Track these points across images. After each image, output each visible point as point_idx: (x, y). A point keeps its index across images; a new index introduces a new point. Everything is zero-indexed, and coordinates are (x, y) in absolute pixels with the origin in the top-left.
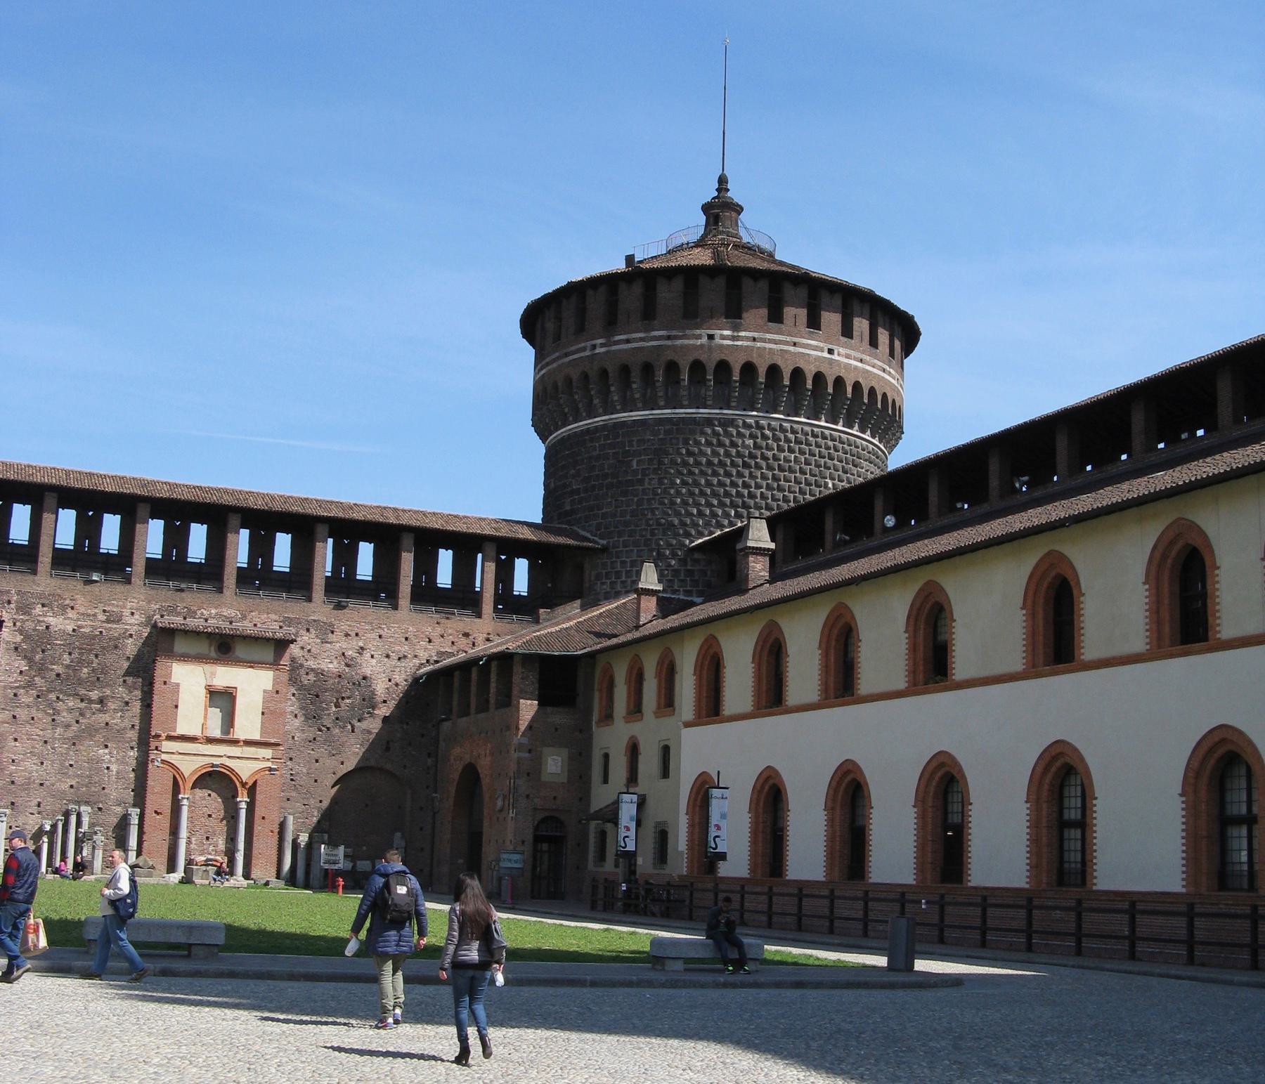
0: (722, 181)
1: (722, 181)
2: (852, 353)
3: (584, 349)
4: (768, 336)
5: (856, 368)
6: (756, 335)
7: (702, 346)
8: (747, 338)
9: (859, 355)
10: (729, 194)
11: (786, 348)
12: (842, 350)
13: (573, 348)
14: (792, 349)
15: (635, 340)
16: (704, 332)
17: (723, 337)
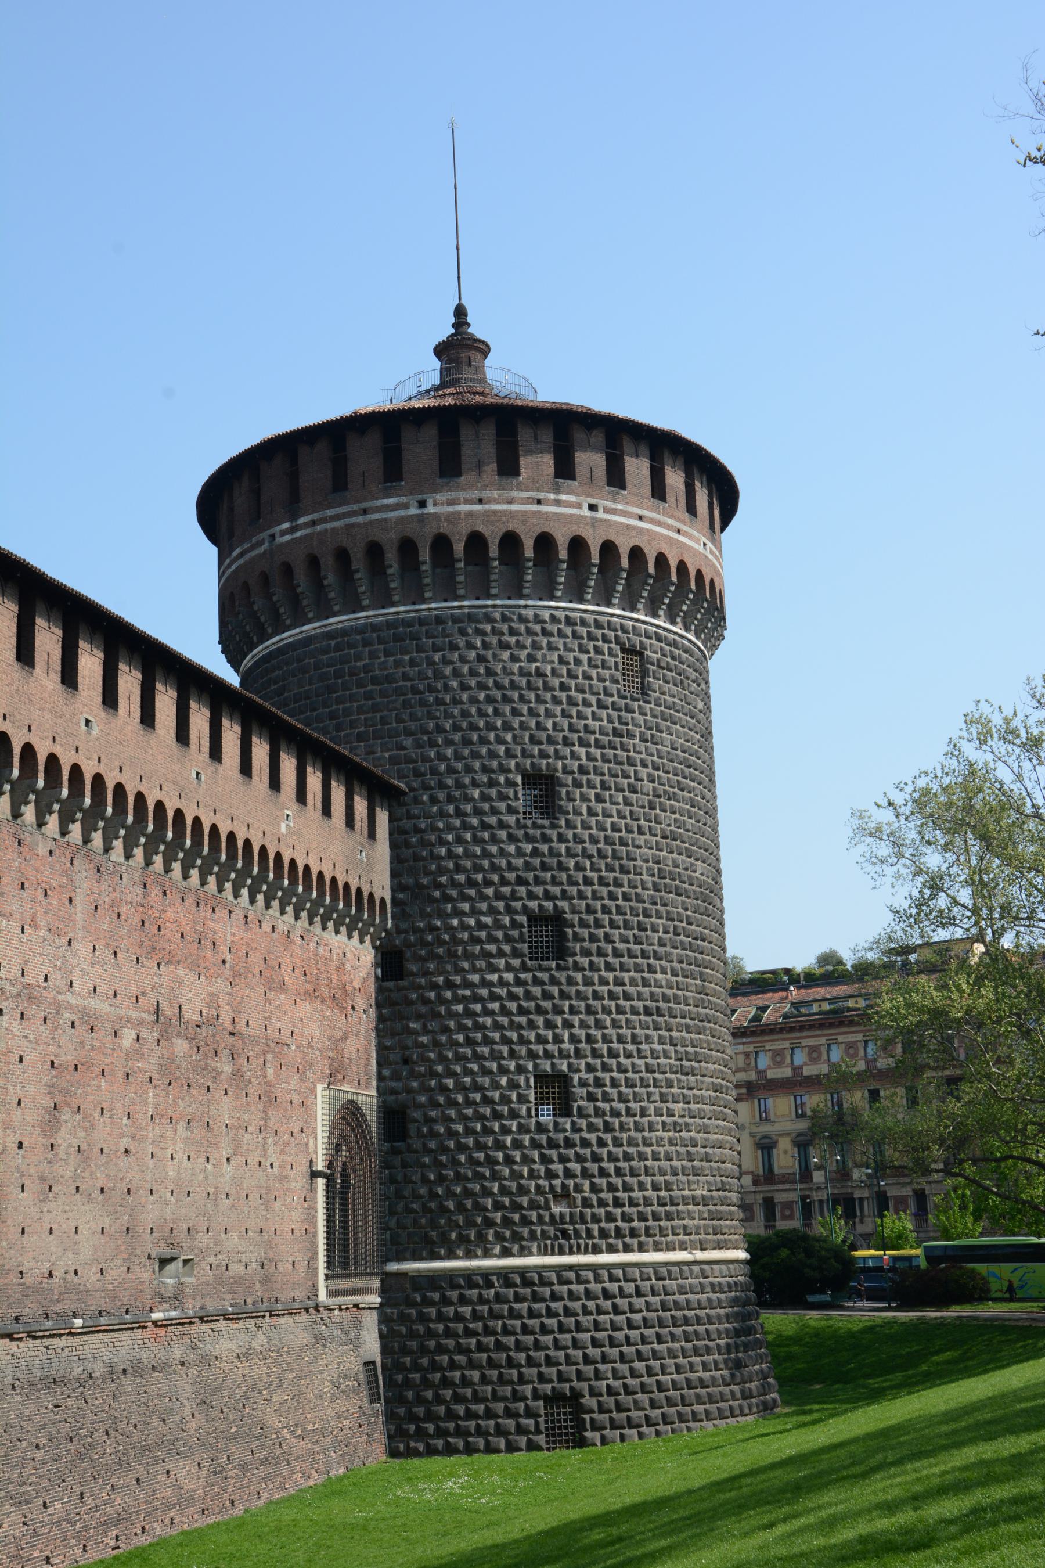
0: (460, 312)
1: (460, 312)
2: (462, 495)
4: (330, 512)
5: (470, 514)
6: (315, 516)
8: (306, 525)
9: (476, 494)
10: (470, 330)
11: (352, 520)
12: (440, 497)
14: (360, 519)
16: (265, 535)
17: (283, 533)
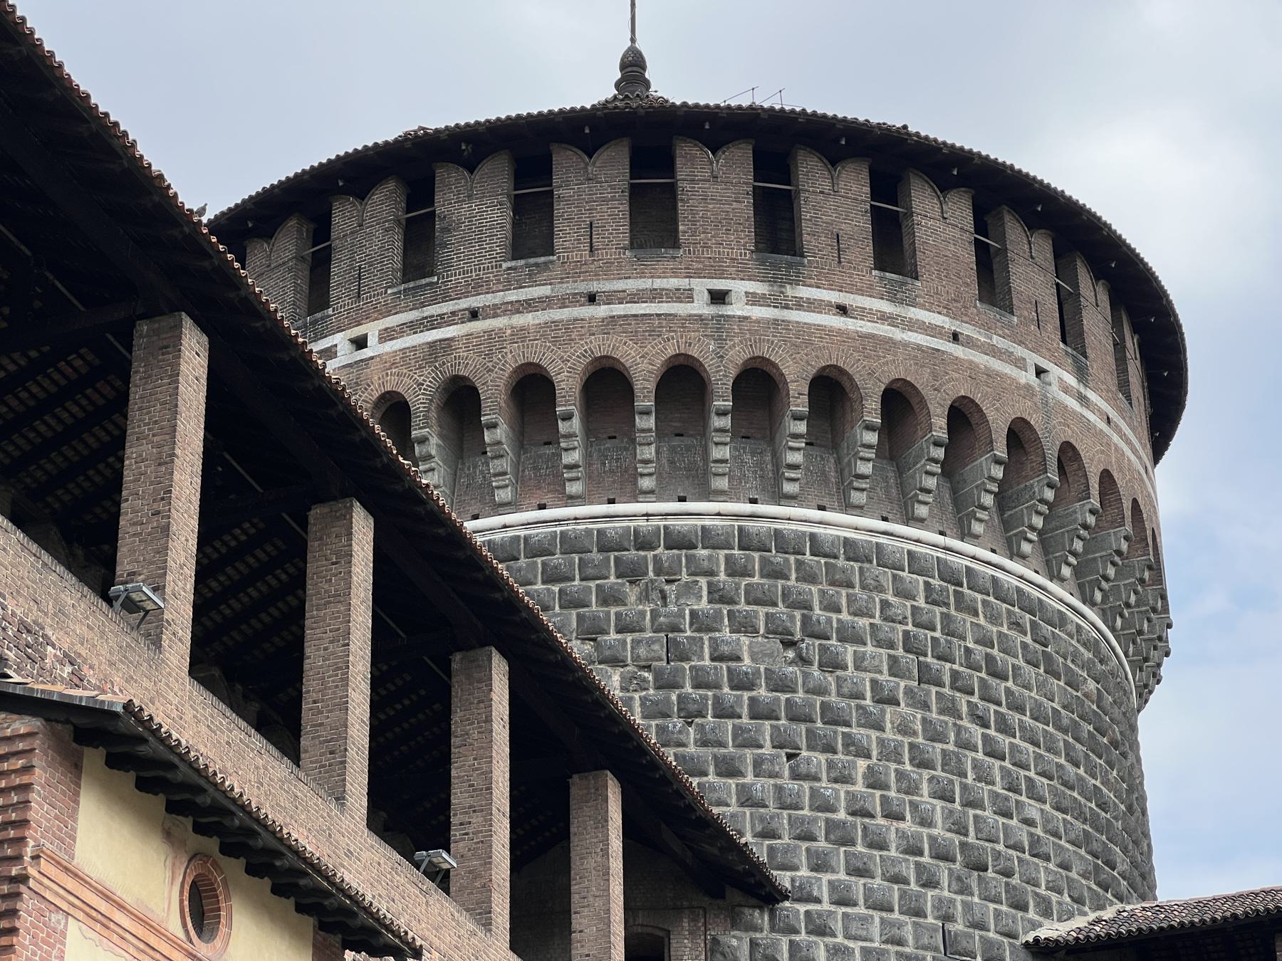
3: (687, 295)
7: (1028, 387)
13: (632, 285)
15: (863, 313)
